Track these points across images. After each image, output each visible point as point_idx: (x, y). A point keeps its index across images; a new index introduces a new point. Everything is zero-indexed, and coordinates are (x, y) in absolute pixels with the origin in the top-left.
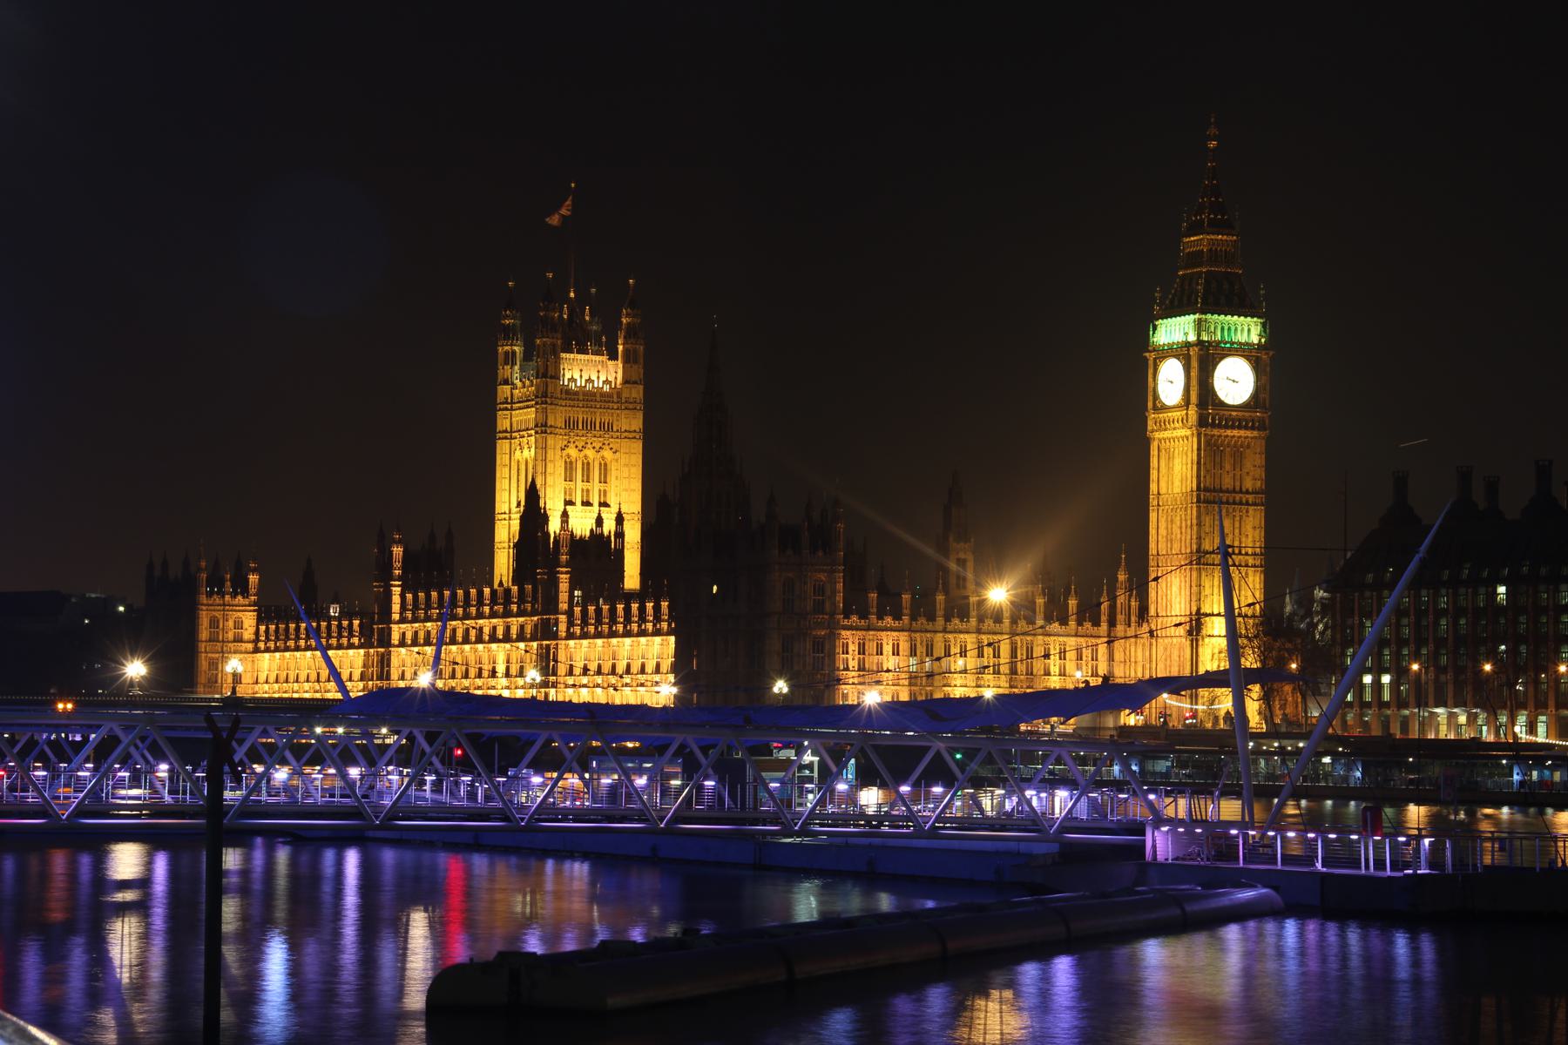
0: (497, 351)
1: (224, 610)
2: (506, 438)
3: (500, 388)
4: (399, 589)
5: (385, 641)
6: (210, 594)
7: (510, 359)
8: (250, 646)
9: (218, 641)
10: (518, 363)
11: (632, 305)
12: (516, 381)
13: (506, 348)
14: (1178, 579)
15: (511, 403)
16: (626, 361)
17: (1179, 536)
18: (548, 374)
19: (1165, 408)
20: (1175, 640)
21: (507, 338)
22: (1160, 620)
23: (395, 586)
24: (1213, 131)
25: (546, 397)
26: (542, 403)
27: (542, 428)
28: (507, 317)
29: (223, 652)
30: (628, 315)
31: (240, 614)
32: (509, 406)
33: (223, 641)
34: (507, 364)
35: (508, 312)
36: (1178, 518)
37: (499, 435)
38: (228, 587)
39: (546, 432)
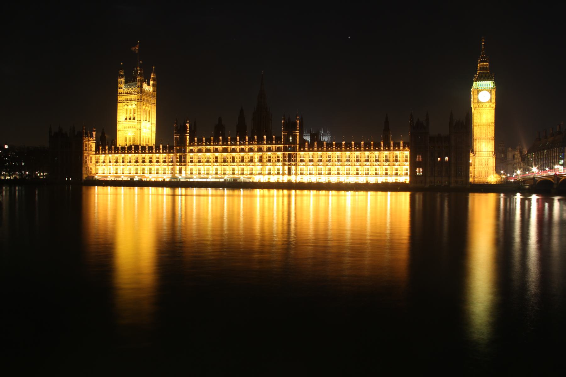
0: (118, 81)
1: (88, 142)
2: (121, 102)
3: (119, 90)
4: (188, 136)
5: (185, 151)
6: (86, 137)
7: (121, 83)
8: (94, 153)
9: (87, 151)
10: (124, 84)
11: (154, 73)
12: (123, 88)
13: (122, 80)
14: (485, 143)
15: (121, 94)
16: (153, 85)
17: (485, 133)
18: (141, 86)
19: (481, 102)
20: (484, 157)
21: (120, 77)
22: (478, 152)
23: (188, 136)
24: (483, 40)
25: (141, 92)
26: (140, 94)
27: (140, 100)
28: (121, 72)
29: (88, 154)
30: (154, 75)
31: (91, 143)
32: (122, 95)
33: (88, 151)
34: (122, 84)
35: (122, 71)
36: (485, 128)
37: (118, 102)
38: (89, 135)
39: (141, 101)
